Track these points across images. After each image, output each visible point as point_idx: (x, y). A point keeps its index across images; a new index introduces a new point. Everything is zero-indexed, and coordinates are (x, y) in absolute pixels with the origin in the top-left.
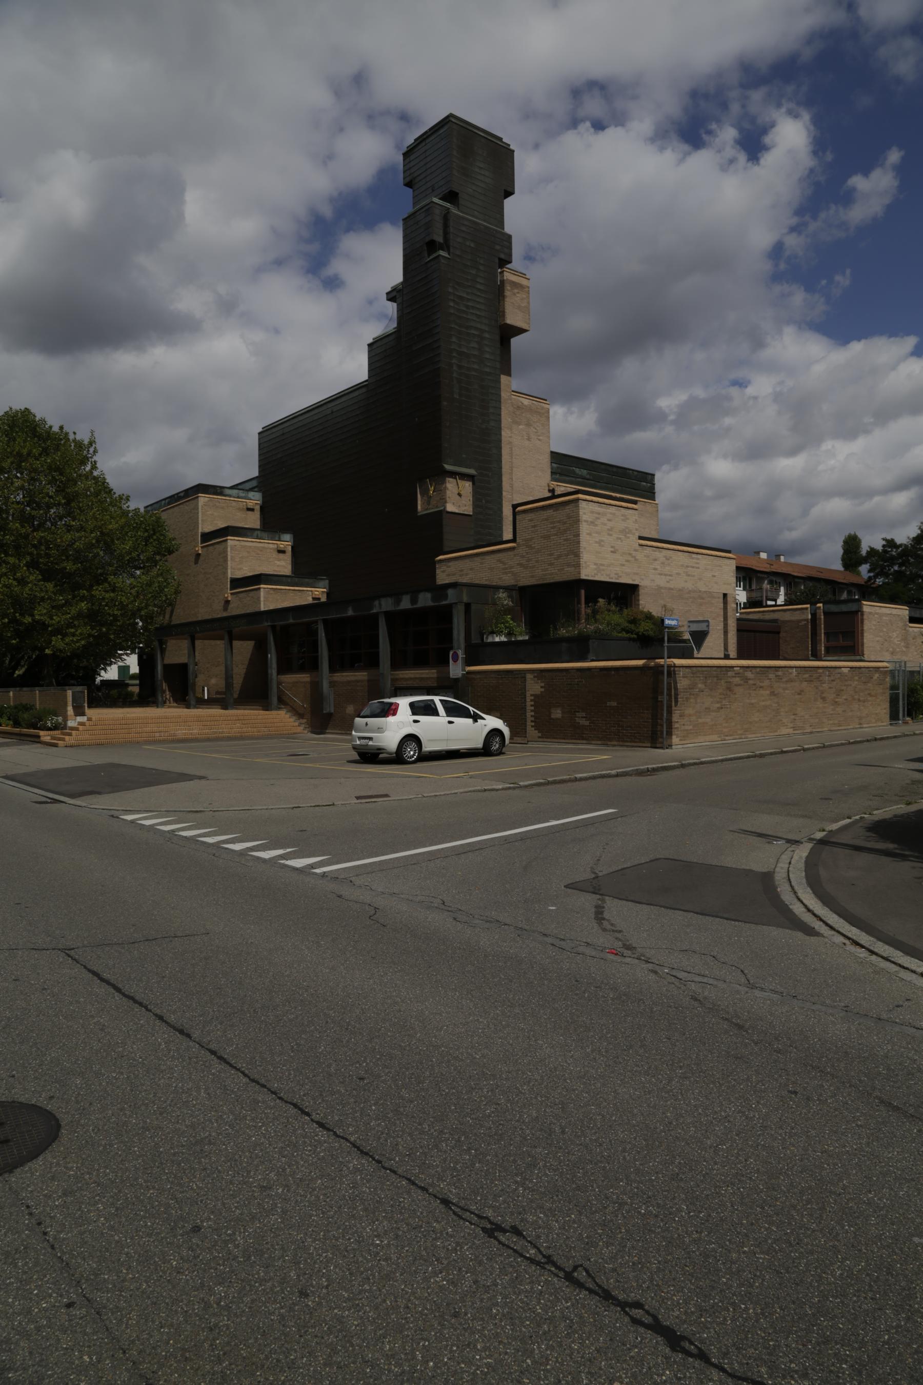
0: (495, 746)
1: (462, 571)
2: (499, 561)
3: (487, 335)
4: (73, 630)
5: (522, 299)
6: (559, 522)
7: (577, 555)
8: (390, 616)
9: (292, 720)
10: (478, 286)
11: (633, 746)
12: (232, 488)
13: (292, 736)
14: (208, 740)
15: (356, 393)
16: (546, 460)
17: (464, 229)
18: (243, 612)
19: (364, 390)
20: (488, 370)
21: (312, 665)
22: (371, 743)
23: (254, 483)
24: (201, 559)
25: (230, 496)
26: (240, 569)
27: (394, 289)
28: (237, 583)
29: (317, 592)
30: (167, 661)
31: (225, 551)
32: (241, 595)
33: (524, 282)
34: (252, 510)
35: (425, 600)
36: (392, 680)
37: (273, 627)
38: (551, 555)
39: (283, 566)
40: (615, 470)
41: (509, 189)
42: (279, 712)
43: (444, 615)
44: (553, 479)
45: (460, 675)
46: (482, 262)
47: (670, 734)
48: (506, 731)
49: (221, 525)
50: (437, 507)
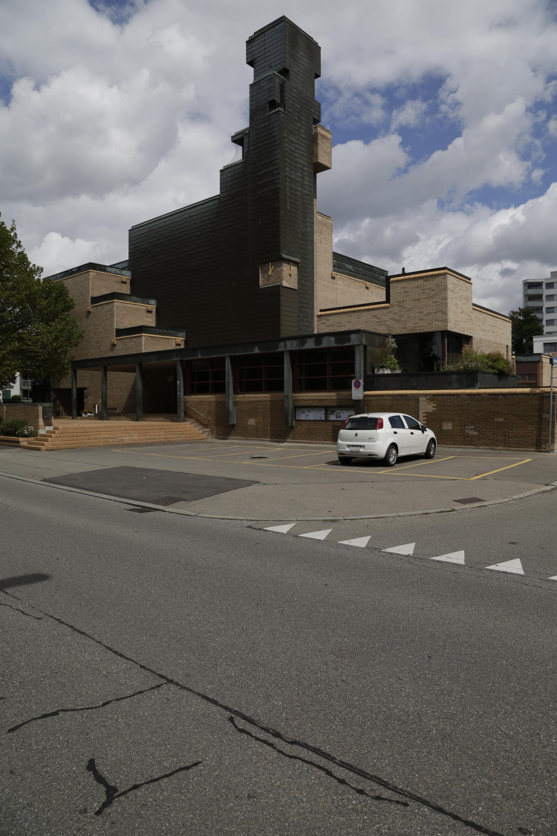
1: (341, 323)
2: (374, 316)
3: (306, 169)
4: (8, 362)
5: (327, 147)
6: (429, 289)
7: (445, 313)
9: (196, 429)
10: (302, 135)
11: (517, 451)
12: (111, 266)
13: (201, 441)
14: (148, 444)
15: (211, 204)
16: (330, 256)
17: (294, 95)
18: (126, 354)
19: (216, 202)
20: (306, 192)
21: (220, 389)
22: (362, 450)
23: (125, 265)
24: (91, 315)
25: (110, 272)
26: (123, 323)
27: (237, 134)
28: (120, 332)
29: (173, 342)
30: (78, 386)
31: (112, 310)
32: (125, 341)
33: (329, 136)
34: (125, 283)
36: (293, 400)
37: (182, 361)
38: (421, 313)
40: (367, 267)
41: (318, 73)
42: (186, 423)
43: (350, 352)
44: (334, 271)
45: (361, 398)
46: (304, 119)
47: (553, 442)
49: (105, 292)
50: (275, 283)
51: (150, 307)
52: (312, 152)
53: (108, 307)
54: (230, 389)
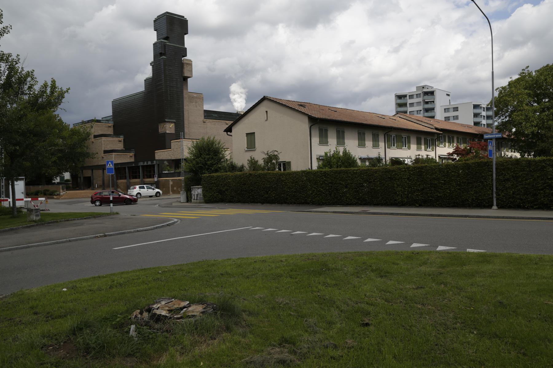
0: (158, 195)
8: (143, 166)
16: (202, 113)
21: (126, 178)
23: (111, 117)
28: (106, 152)
33: (190, 62)
35: (149, 163)
39: (120, 146)
48: (161, 192)
49: (101, 133)
51: (120, 139)
52: (182, 72)
53: (100, 141)
54: (128, 177)
